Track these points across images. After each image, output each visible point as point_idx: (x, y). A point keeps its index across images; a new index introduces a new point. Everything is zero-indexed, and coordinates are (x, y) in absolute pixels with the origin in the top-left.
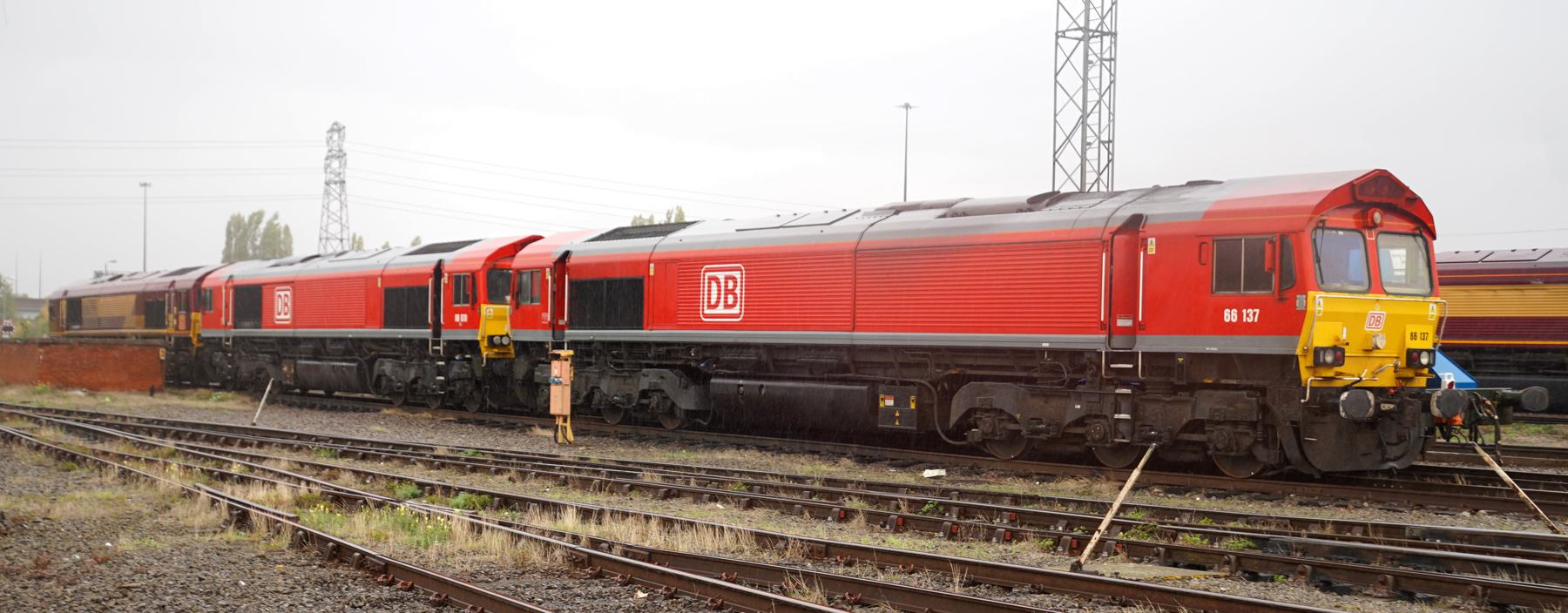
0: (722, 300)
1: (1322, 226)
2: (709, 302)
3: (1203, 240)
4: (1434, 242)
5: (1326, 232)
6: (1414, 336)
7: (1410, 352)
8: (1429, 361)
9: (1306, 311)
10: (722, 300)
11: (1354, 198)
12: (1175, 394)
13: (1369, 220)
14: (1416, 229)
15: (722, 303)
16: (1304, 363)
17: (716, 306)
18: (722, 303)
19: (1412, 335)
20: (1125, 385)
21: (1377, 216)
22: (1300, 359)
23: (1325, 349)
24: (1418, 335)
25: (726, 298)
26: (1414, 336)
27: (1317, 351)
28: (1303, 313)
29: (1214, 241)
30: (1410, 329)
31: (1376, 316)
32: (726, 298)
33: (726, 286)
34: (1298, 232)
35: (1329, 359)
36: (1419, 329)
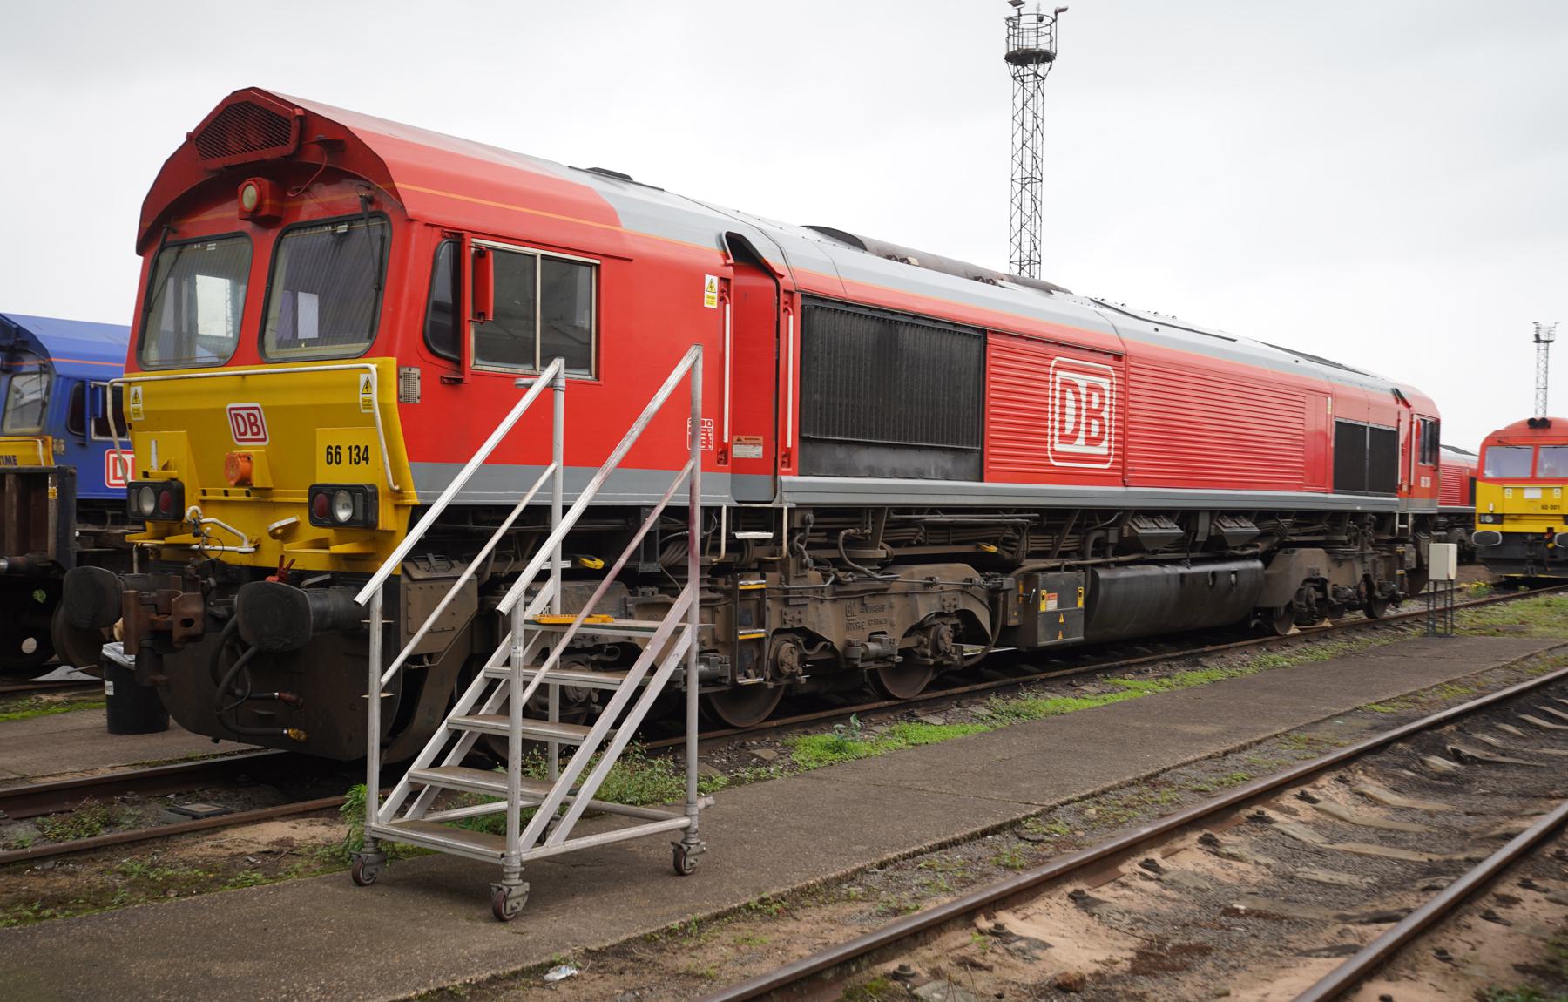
0: (1083, 427)
2: (1062, 429)
6: (333, 455)
7: (315, 490)
8: (354, 514)
10: (1083, 427)
15: (1082, 435)
17: (1071, 439)
18: (1082, 435)
19: (328, 453)
24: (345, 453)
25: (1088, 424)
26: (333, 455)
30: (326, 437)
31: (244, 413)
32: (1088, 424)
33: (1089, 402)
36: (345, 438)
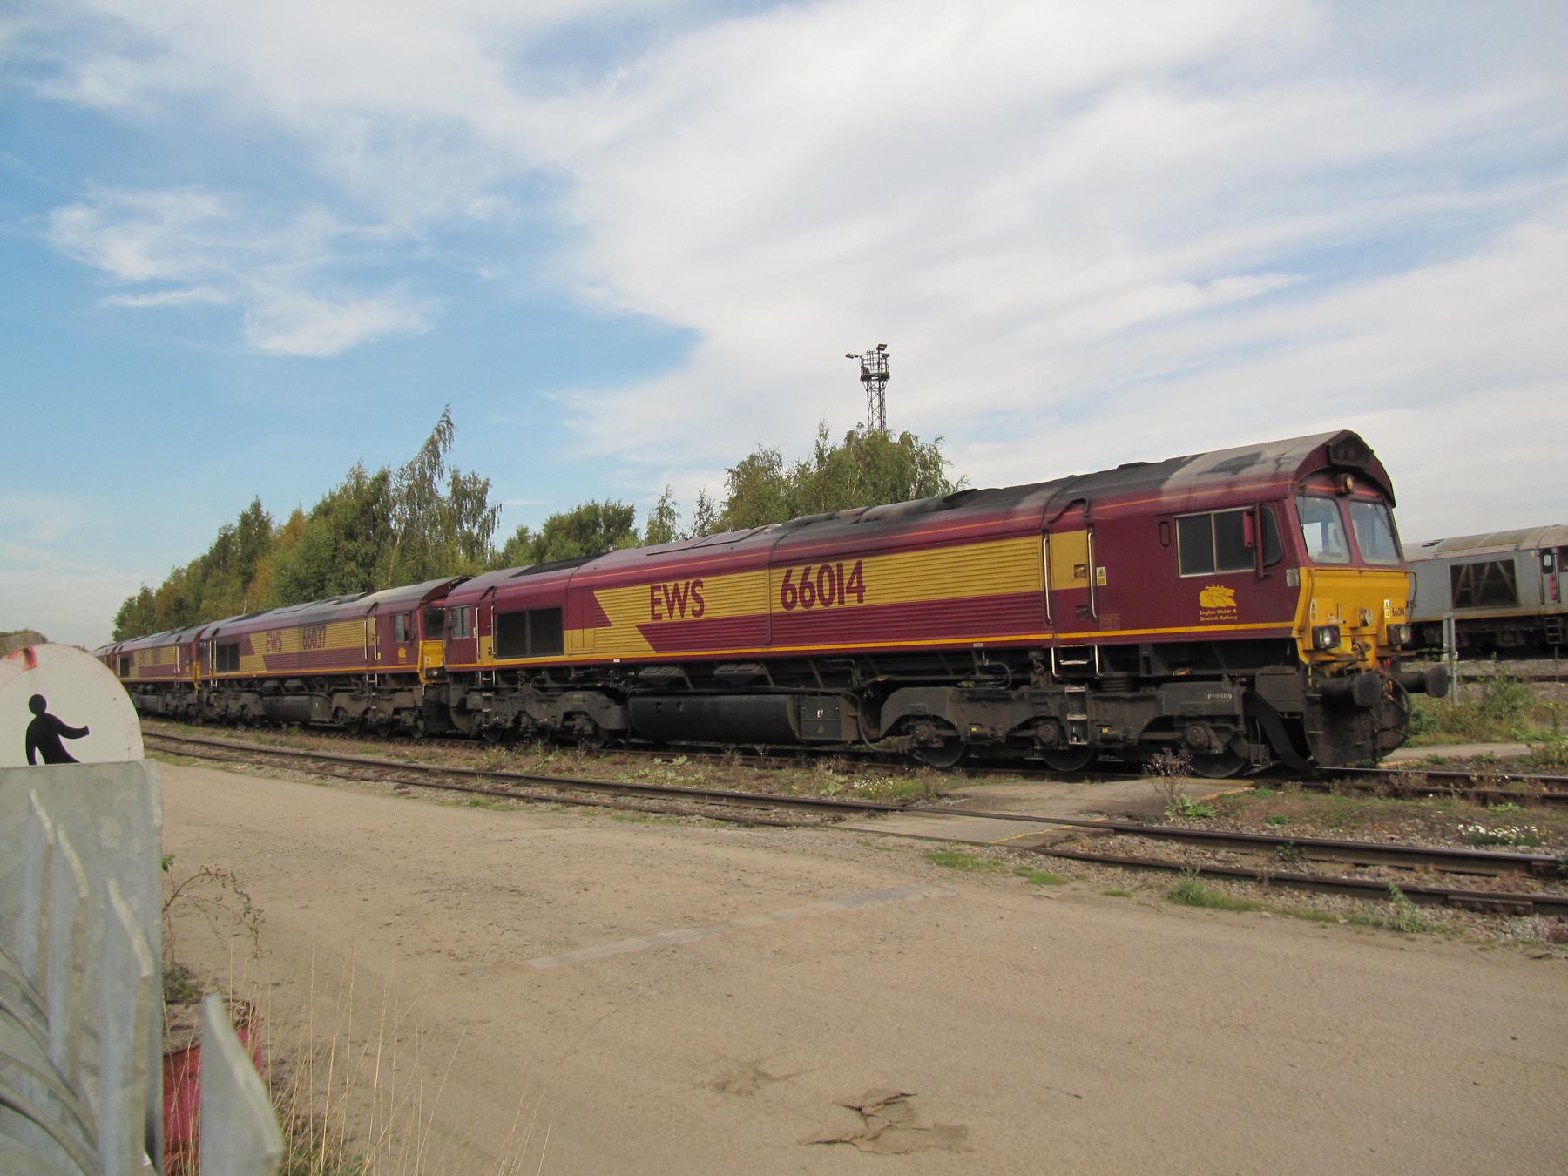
1: (1302, 492)
3: (1163, 519)
4: (1394, 510)
5: (1307, 499)
9: (1300, 587)
11: (1329, 461)
12: (1136, 689)
13: (1343, 488)
14: (1378, 497)
16: (1304, 645)
20: (1077, 682)
21: (1350, 482)
22: (1299, 644)
23: (1322, 629)
27: (1316, 632)
28: (1297, 589)
29: (1176, 519)
34: (1278, 500)
35: (1327, 640)
